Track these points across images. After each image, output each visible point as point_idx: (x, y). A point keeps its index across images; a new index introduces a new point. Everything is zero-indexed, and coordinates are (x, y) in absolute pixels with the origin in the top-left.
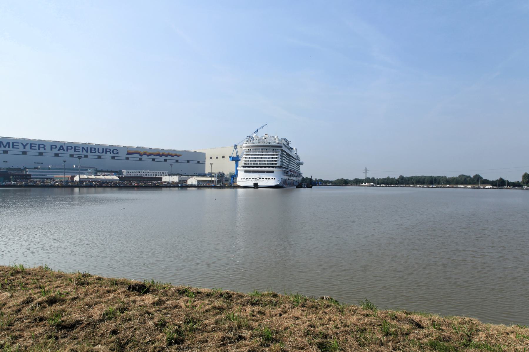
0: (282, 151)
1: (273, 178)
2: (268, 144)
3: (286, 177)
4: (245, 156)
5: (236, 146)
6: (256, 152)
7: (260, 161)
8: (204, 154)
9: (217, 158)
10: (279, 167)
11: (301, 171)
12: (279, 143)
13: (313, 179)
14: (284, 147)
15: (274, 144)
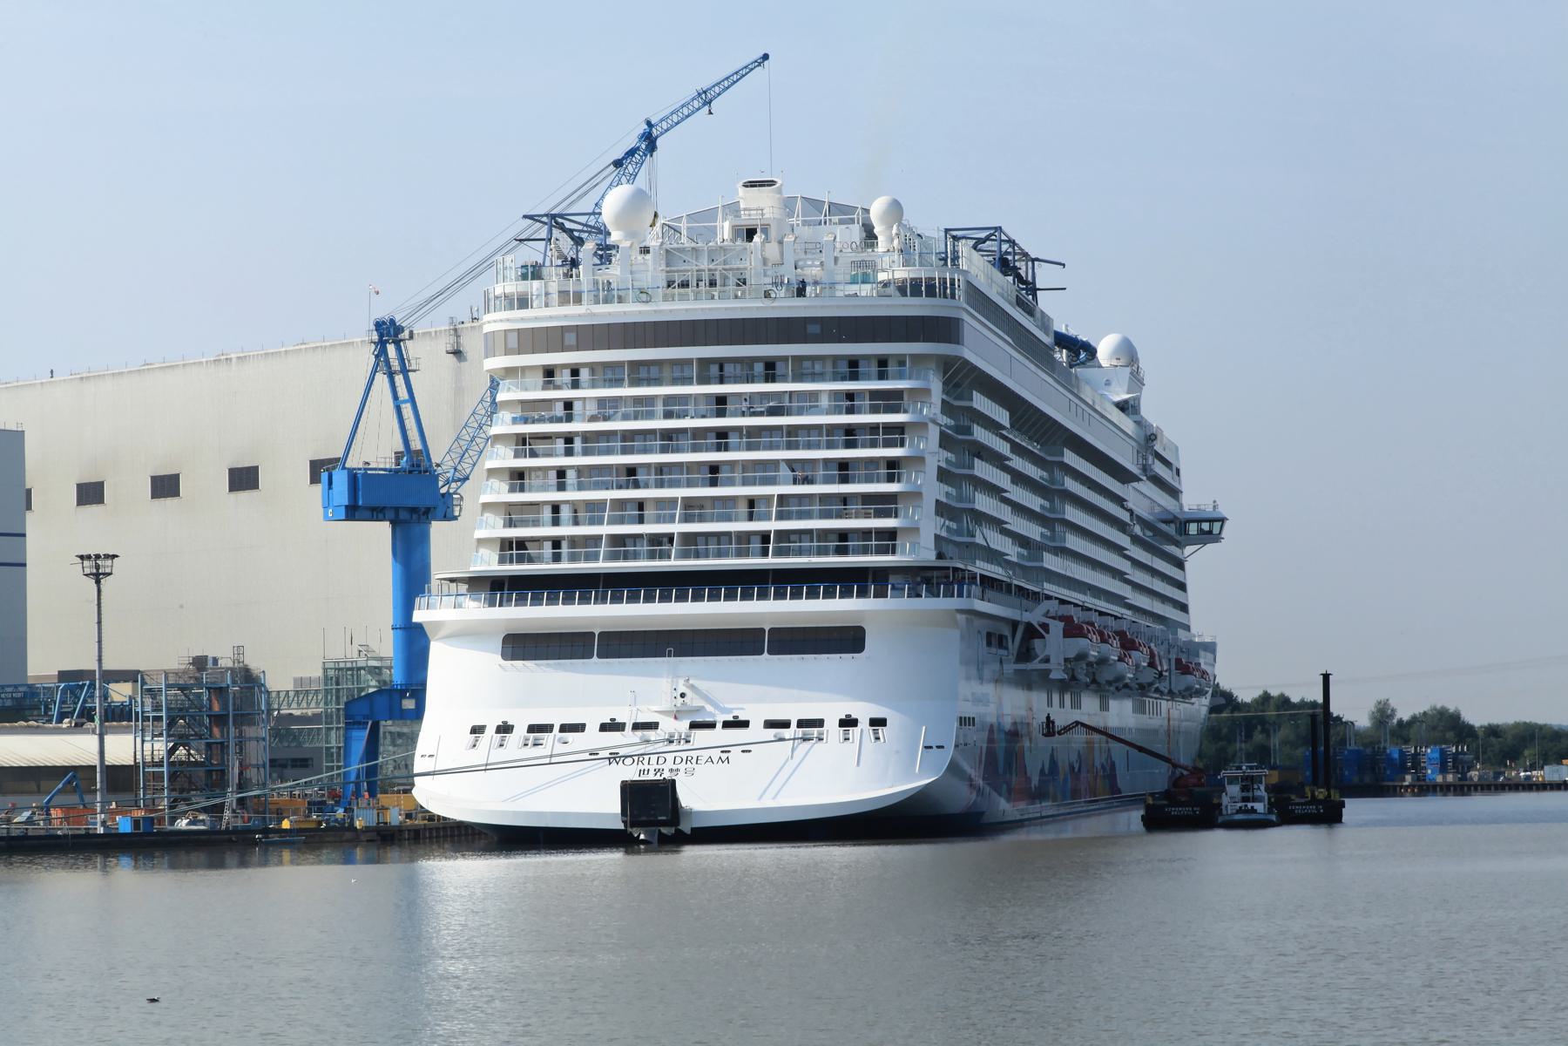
0: (962, 379)
1: (864, 711)
2: (785, 306)
3: (1013, 704)
4: (505, 458)
5: (388, 333)
6: (643, 406)
7: (692, 509)
8: (19, 435)
9: (166, 486)
10: (922, 579)
11: (1201, 625)
12: (913, 288)
13: (1354, 709)
14: (974, 326)
15: (863, 299)
